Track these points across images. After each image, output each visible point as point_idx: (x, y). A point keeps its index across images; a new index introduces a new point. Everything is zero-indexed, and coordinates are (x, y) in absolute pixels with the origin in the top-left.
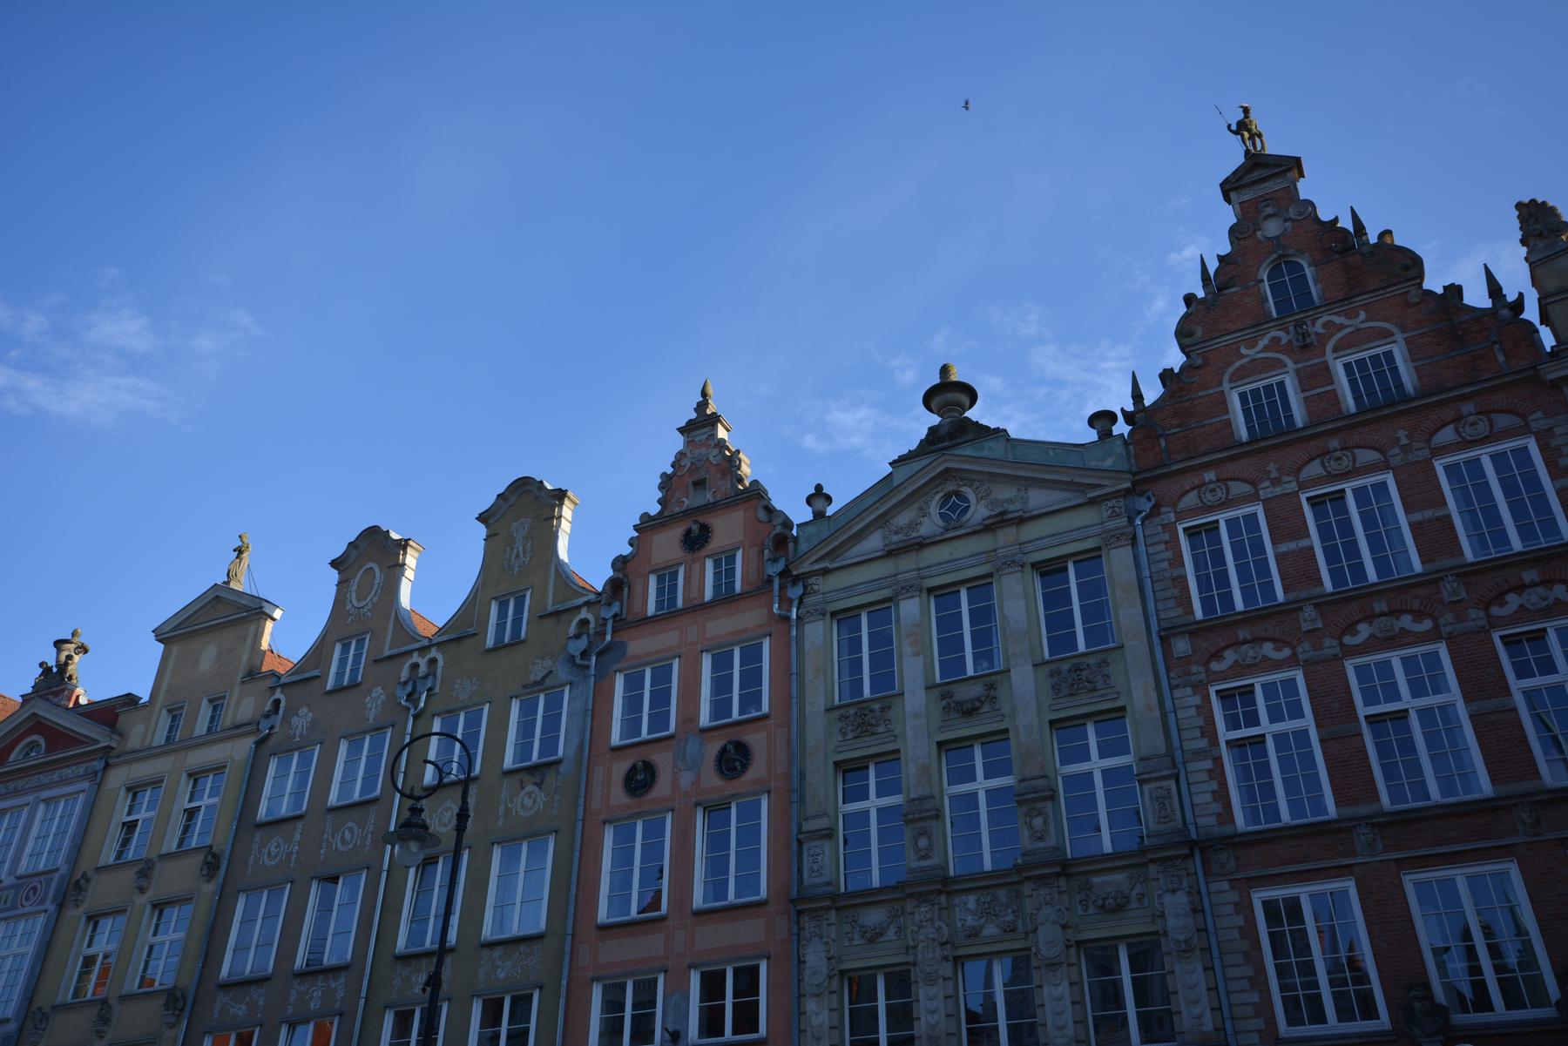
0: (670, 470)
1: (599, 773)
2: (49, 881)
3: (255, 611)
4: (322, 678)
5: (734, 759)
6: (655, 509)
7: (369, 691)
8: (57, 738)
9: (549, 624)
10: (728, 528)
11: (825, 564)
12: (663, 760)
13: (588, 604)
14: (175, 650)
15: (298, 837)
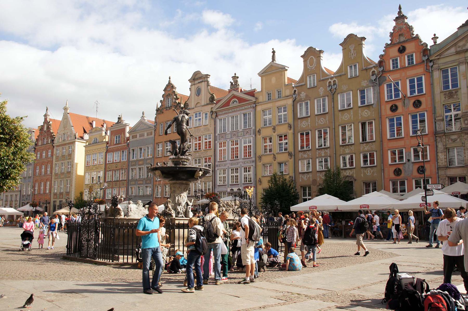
0: (392, 31)
1: (383, 107)
2: (251, 130)
3: (283, 69)
4: (306, 84)
5: (417, 104)
6: (389, 42)
7: (319, 88)
8: (241, 100)
9: (365, 71)
10: (410, 47)
11: (438, 57)
12: (399, 104)
13: (374, 67)
14: (264, 78)
15: (309, 121)
